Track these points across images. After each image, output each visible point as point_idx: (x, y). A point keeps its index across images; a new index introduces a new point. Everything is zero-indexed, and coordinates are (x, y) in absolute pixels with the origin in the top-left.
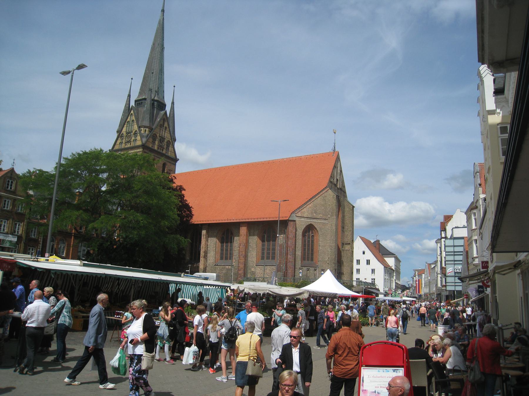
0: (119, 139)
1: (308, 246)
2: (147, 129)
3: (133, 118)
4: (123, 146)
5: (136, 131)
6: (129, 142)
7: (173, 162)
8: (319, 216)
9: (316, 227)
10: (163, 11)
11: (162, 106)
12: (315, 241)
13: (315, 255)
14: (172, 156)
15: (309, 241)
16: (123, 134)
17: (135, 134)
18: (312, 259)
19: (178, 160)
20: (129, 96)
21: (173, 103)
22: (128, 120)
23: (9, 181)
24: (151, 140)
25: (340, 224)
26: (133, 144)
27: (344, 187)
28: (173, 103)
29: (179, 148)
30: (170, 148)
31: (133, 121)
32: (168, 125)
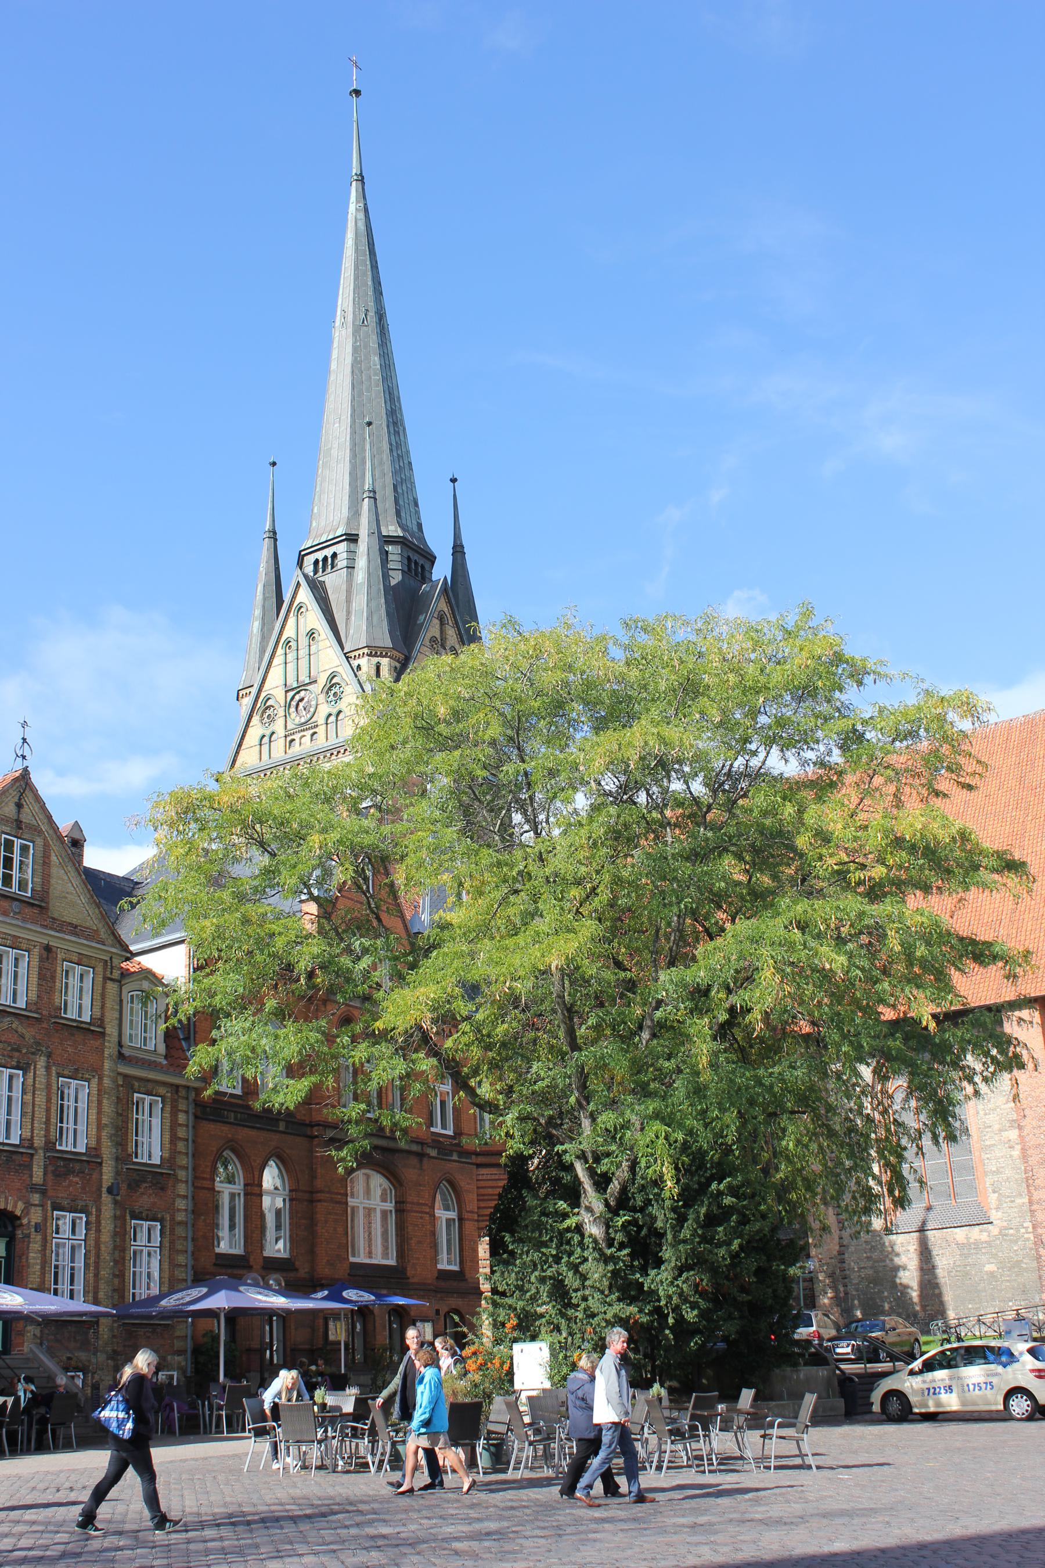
0: (256, 719)
2: (385, 662)
3: (314, 618)
5: (333, 676)
17: (332, 687)
21: (458, 551)
22: (289, 632)
23: (9, 846)
28: (458, 551)
31: (311, 634)
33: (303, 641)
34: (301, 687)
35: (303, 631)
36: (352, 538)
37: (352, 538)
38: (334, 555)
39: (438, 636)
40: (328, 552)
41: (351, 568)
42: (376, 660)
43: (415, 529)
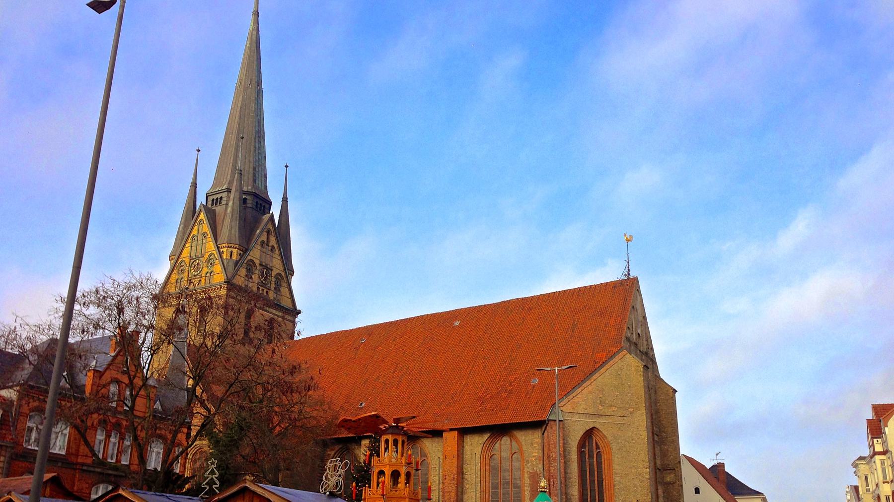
0: (175, 271)
1: (592, 474)
2: (235, 251)
3: (206, 228)
5: (210, 255)
7: (290, 318)
8: (608, 412)
9: (605, 433)
10: (257, 14)
11: (264, 204)
12: (605, 466)
15: (591, 465)
19: (299, 312)
20: (194, 185)
21: (285, 200)
22: (195, 232)
24: (243, 272)
27: (652, 349)
28: (285, 200)
29: (301, 288)
30: (284, 290)
33: (200, 237)
34: (197, 257)
36: (229, 190)
37: (229, 190)
38: (221, 198)
40: (219, 196)
41: (227, 204)
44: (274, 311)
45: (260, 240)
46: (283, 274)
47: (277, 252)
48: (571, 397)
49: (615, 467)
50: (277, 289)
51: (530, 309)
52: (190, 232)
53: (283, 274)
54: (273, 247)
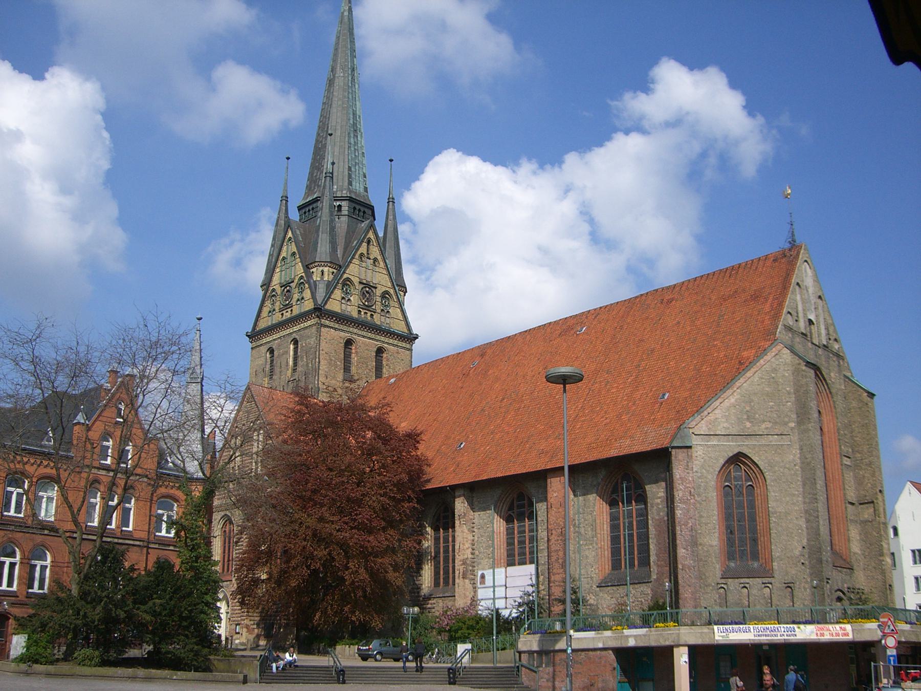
2: (326, 269)
4: (277, 318)
5: (302, 277)
6: (288, 306)
9: (756, 459)
12: (758, 503)
13: (761, 540)
14: (400, 327)
16: (274, 290)
18: (755, 556)
20: (285, 199)
22: (283, 254)
25: (275, 254)
26: (296, 310)
30: (395, 311)
32: (382, 253)
35: (290, 254)
39: (365, 252)
42: (321, 268)
43: (362, 190)
44: (383, 339)
45: (359, 252)
46: (392, 291)
47: (382, 264)
48: (706, 413)
49: (772, 504)
50: (385, 312)
51: (670, 301)
52: (279, 254)
53: (392, 291)
54: (375, 260)
